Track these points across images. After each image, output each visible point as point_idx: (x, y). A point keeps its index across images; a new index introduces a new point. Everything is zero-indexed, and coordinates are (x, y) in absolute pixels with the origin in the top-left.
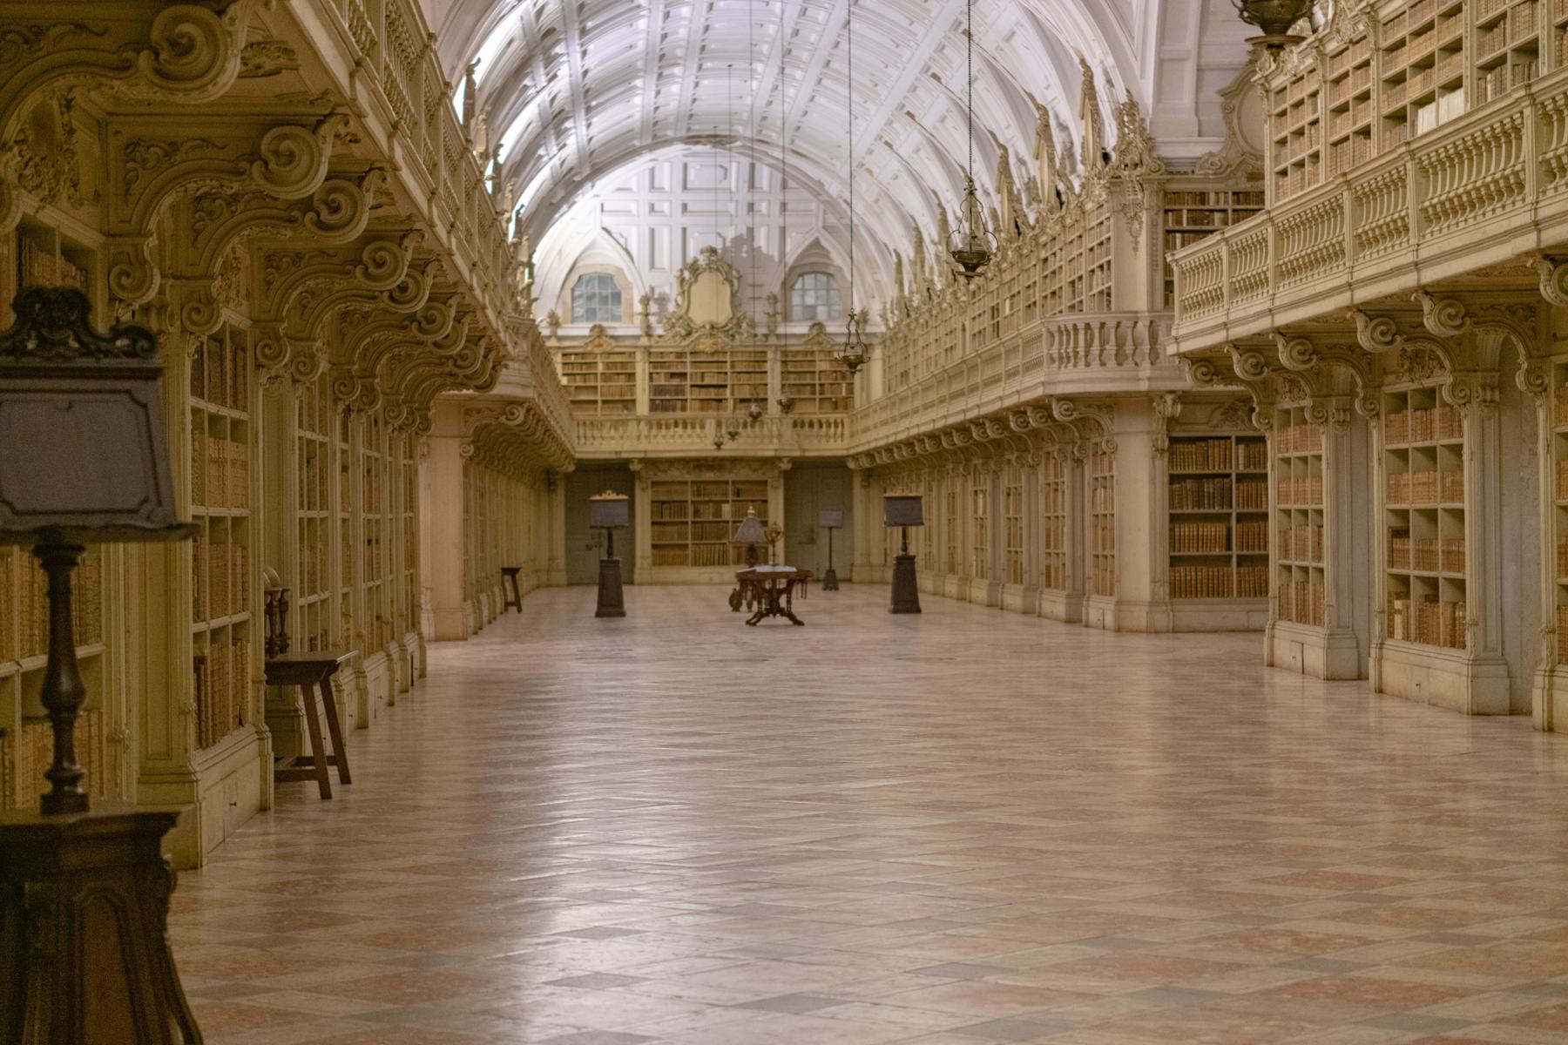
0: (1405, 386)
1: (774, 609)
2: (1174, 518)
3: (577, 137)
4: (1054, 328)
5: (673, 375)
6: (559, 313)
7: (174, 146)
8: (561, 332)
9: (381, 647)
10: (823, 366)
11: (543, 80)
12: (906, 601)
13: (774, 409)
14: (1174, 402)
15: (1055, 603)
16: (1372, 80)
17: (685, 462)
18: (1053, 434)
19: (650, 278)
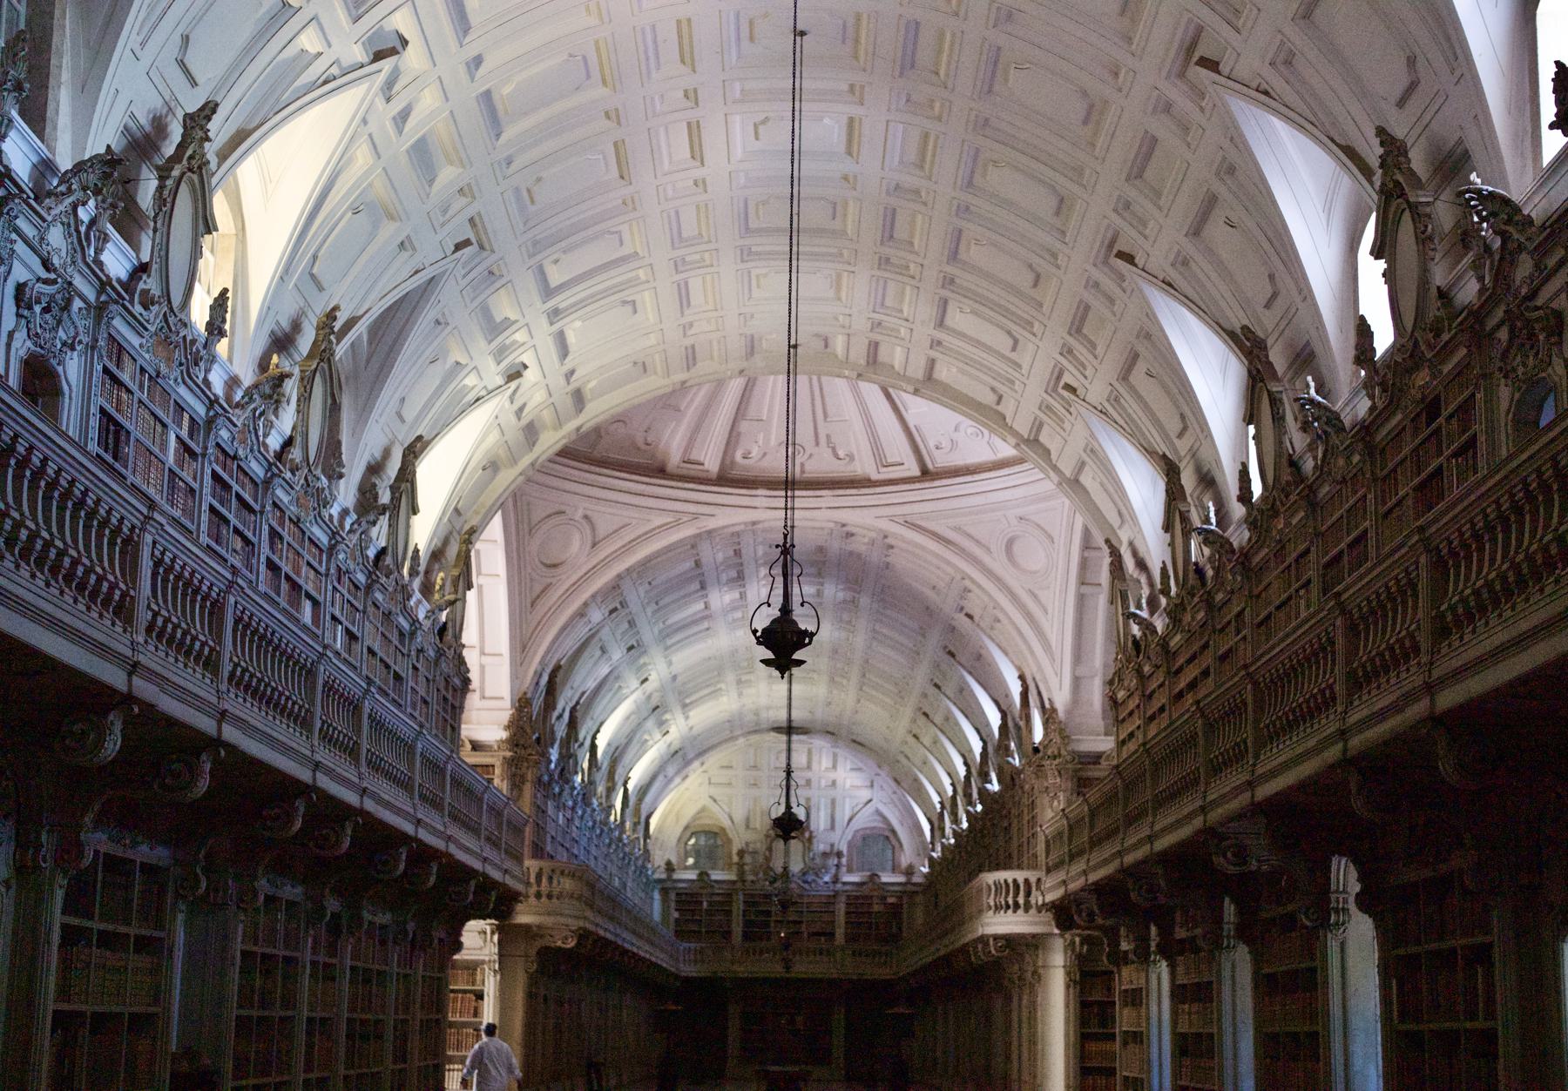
0: (1181, 933)
3: (679, 727)
4: (991, 882)
5: (763, 912)
6: (674, 860)
8: (676, 876)
10: (876, 908)
11: (635, 683)
14: (1082, 944)
19: (749, 836)
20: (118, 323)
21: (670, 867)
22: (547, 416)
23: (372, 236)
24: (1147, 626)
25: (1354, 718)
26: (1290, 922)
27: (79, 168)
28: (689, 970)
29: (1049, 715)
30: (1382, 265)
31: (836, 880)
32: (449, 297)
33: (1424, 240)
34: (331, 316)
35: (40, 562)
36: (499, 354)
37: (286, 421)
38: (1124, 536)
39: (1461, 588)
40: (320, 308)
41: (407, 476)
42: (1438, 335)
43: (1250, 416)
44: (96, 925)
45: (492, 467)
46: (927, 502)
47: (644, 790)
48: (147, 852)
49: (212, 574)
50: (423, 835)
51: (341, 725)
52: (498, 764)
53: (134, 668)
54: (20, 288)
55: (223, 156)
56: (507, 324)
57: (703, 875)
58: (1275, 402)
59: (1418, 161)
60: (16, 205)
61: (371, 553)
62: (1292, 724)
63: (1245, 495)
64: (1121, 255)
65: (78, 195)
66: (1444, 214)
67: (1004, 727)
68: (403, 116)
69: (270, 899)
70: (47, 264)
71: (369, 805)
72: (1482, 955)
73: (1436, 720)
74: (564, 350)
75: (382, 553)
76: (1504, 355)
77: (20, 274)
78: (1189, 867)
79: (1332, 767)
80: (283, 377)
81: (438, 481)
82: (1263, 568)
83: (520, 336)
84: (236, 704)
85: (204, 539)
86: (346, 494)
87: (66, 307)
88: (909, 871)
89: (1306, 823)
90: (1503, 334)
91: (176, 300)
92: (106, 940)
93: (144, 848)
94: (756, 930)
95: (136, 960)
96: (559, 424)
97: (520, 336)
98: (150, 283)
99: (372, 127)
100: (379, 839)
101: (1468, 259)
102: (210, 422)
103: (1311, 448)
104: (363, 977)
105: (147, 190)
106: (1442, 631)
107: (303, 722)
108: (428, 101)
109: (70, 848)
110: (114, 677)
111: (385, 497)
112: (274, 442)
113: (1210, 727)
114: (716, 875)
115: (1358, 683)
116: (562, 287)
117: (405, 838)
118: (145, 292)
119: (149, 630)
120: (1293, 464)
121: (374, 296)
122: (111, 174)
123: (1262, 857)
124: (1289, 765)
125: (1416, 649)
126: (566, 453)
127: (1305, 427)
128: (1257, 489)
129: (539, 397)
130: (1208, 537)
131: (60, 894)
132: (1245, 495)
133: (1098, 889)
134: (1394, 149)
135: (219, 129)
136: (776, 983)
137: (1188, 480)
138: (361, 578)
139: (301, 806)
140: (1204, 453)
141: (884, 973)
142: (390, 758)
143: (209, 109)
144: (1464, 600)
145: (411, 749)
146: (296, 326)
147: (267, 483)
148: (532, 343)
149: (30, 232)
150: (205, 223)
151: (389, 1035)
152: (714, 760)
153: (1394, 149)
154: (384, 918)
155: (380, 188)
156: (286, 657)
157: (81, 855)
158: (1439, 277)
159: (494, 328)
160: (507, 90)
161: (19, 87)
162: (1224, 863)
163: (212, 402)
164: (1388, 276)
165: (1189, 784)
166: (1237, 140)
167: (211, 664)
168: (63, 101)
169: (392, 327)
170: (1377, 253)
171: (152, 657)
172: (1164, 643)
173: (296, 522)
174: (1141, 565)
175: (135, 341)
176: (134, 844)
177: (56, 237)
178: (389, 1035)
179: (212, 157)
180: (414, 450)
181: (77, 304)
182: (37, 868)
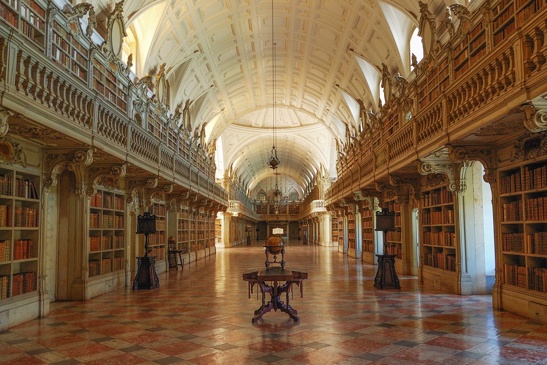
0: (349, 211)
2: (333, 230)
7: (136, 182)
13: (288, 213)
24: (343, 155)
26: (368, 209)
27: (142, 79)
28: (259, 220)
30: (383, 89)
31: (287, 202)
32: (209, 96)
33: (390, 85)
35: (142, 153)
37: (181, 121)
38: (339, 137)
39: (394, 151)
40: (186, 99)
41: (203, 130)
43: (361, 116)
46: (302, 131)
49: (171, 153)
50: (210, 197)
51: (194, 179)
52: (222, 182)
54: (134, 102)
57: (261, 201)
58: (365, 114)
59: (389, 70)
61: (197, 145)
62: (366, 175)
63: (360, 131)
66: (394, 80)
67: (317, 173)
70: (138, 97)
71: (200, 192)
73: (389, 174)
77: (133, 99)
78: (349, 199)
81: (208, 130)
84: (177, 176)
85: (168, 145)
86: (192, 134)
88: (300, 200)
89: (368, 192)
90: (403, 103)
91: (161, 101)
98: (156, 98)
100: (202, 199)
102: (168, 123)
103: (371, 122)
105: (154, 81)
109: (148, 202)
110: (156, 173)
111: (199, 135)
112: (179, 126)
113: (352, 174)
116: (231, 93)
117: (206, 198)
123: (362, 198)
124: (366, 182)
128: (362, 130)
130: (353, 138)
132: (360, 131)
133: (334, 203)
134: (385, 67)
136: (277, 222)
138: (196, 150)
140: (353, 122)
141: (296, 219)
142: (203, 183)
143: (164, 65)
146: (182, 103)
147: (178, 133)
149: (135, 91)
157: (150, 203)
158: (393, 92)
162: (356, 199)
164: (384, 91)
166: (357, 64)
167: (172, 169)
169: (199, 103)
173: (184, 140)
174: (342, 142)
175: (154, 109)
177: (139, 92)
179: (165, 73)
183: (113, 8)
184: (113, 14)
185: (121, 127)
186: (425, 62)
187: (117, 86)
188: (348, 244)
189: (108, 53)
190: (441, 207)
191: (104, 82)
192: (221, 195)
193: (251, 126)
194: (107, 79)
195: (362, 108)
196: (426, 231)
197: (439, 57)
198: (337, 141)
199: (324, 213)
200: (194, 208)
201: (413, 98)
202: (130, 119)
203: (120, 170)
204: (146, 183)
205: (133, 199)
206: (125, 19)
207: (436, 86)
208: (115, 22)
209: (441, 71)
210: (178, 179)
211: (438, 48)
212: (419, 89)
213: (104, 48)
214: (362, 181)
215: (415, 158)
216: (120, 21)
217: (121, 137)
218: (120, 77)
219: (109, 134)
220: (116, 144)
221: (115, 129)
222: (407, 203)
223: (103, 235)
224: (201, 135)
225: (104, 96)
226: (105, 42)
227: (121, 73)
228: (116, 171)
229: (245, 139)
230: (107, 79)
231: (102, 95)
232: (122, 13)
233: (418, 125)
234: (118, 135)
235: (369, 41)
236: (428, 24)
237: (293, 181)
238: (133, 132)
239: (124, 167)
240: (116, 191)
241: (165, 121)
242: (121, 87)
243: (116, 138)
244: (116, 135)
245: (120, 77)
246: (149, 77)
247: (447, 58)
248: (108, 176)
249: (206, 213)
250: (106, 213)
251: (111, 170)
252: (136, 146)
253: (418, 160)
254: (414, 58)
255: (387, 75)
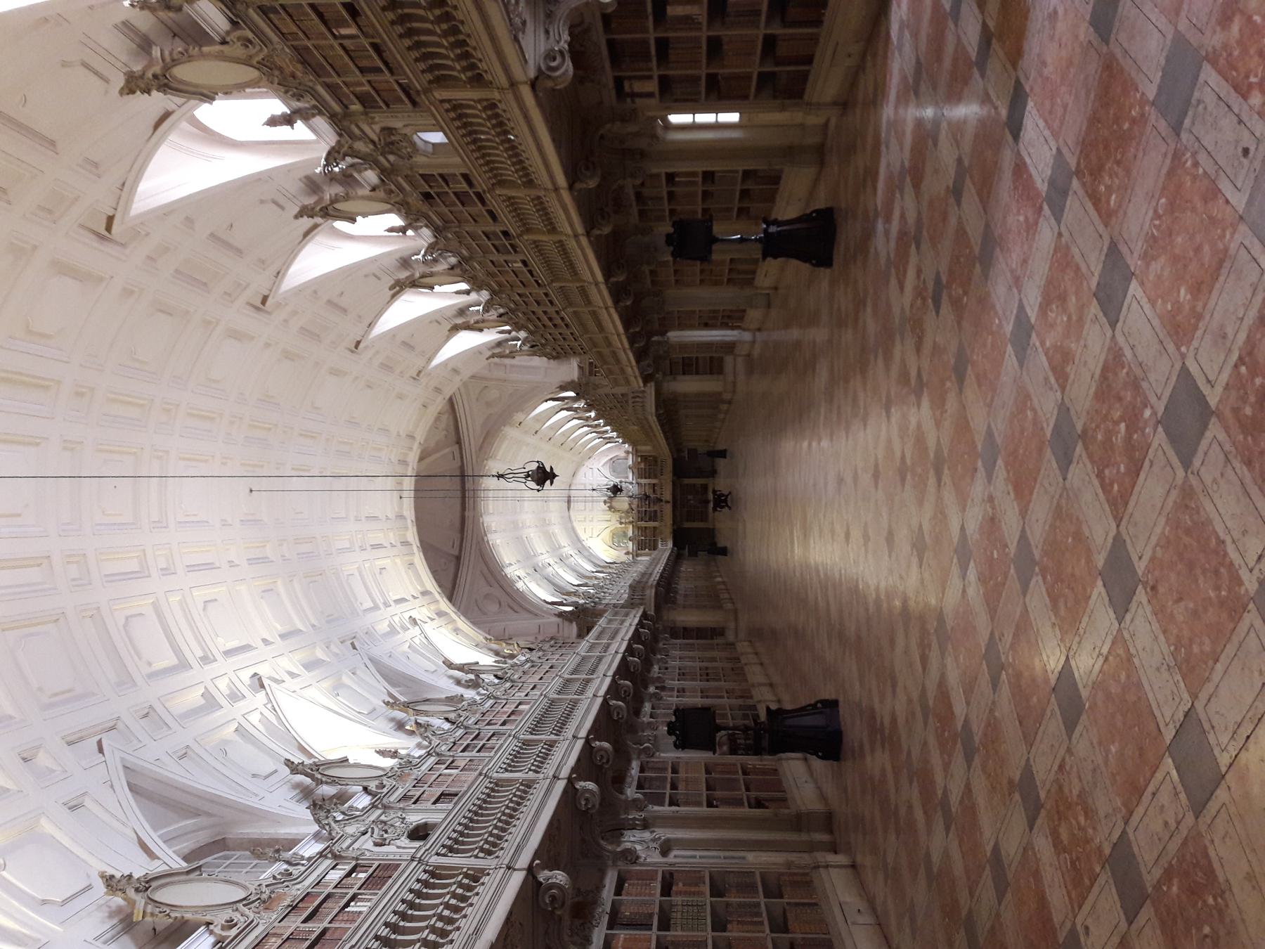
1: (725, 501)
2: (697, 373)
3: (568, 550)
9: (742, 668)
10: (642, 466)
12: (722, 454)
15: (724, 407)
16: (553, 331)
17: (674, 511)
18: (669, 412)
20: (392, 799)
21: (627, 553)
22: (433, 607)
23: (349, 687)
25: (569, 231)
27: (318, 821)
28: (670, 544)
29: (563, 388)
30: (359, 218)
32: (379, 651)
33: (347, 198)
34: (387, 703)
36: (405, 629)
37: (437, 722)
39: (510, 173)
41: (461, 668)
42: (391, 191)
44: (668, 791)
45: (457, 630)
47: (596, 565)
48: (634, 770)
49: (509, 745)
51: (576, 686)
53: (555, 777)
54: (376, 844)
55: (311, 756)
56: (390, 625)
58: (422, 277)
59: (310, 201)
60: (336, 848)
61: (496, 681)
62: (571, 266)
63: (467, 292)
64: (356, 347)
65: (330, 820)
67: (568, 409)
68: (293, 675)
69: (651, 717)
70: (364, 833)
71: (611, 673)
72: (671, 177)
73: (571, 187)
74: (403, 600)
75: (496, 676)
76: (400, 157)
79: (590, 242)
80: (417, 723)
82: (500, 285)
83: (396, 619)
86: (469, 694)
87: (385, 823)
88: (627, 452)
90: (392, 158)
92: (674, 786)
93: (633, 772)
94: (653, 517)
95: (682, 775)
96: (437, 601)
97: (396, 619)
98: (372, 786)
99: (297, 688)
100: (624, 669)
101: (356, 175)
102: (438, 754)
103: (445, 258)
104: (682, 675)
105: (328, 790)
106: (530, 183)
107: (575, 703)
108: (286, 663)
109: (636, 805)
110: (560, 786)
111: (472, 677)
112: (447, 726)
114: (630, 533)
115: (553, 229)
116: (373, 601)
117: (624, 659)
118: (377, 787)
119: (537, 772)
120: (452, 268)
121: (376, 684)
122: (318, 806)
125: (539, 198)
126: (450, 599)
127: (435, 261)
129: (424, 610)
131: (656, 808)
132: (467, 292)
135: (297, 758)
137: (459, 321)
139: (613, 702)
141: (670, 462)
142: (589, 666)
144: (517, 171)
145: (584, 658)
146: (392, 720)
147: (466, 728)
148: (400, 614)
149: (349, 841)
150: (344, 761)
151: (705, 664)
152: (583, 536)
153: (304, 212)
154: (656, 668)
155: (326, 684)
156: (547, 712)
158: (366, 191)
159: (393, 631)
160: (278, 627)
161: (278, 851)
163: (429, 754)
164: (365, 215)
165: (594, 314)
166: (300, 290)
167: (551, 744)
168: (285, 831)
169: (391, 676)
170: (353, 220)
171: (549, 770)
172: (531, 332)
173: (484, 714)
176: (631, 776)
177: (351, 829)
178: (705, 664)
180: (450, 665)
181: (383, 818)
182: (644, 819)
183: (118, 901)
184: (132, 903)
185: (434, 886)
186: (286, 85)
187: (329, 890)
188: (733, 328)
189: (237, 917)
190: (658, 40)
191: (316, 927)
192: (614, 626)
193: (458, 558)
194: (305, 921)
195: (414, 284)
196: (717, 97)
197: (265, 41)
198: (493, 356)
199: (658, 393)
200: (646, 688)
201: (377, 128)
202: (413, 859)
203: (553, 886)
204: (586, 812)
205: (628, 845)
206: (155, 868)
207: (342, 52)
208: (160, 896)
209: (301, 34)
210: (578, 728)
211: (239, 39)
212: (353, 107)
213: (223, 928)
214: (587, 276)
215: (526, 92)
216: (154, 884)
217: (461, 885)
218: (307, 883)
219: (450, 921)
220: (480, 901)
221: (437, 905)
222: (643, 154)
223: (724, 930)
224: (472, 671)
225: (353, 926)
226: (208, 924)
227: (297, 880)
228: (553, 897)
229: (486, 571)
230: (305, 921)
231: (350, 932)
232: (136, 876)
233: (441, 81)
234: (454, 895)
235: (239, 252)
236: (183, 72)
237: (583, 470)
238: (451, 849)
239: (543, 875)
240: (607, 894)
241: (432, 760)
242: (335, 876)
243: (463, 899)
244: (453, 902)
245: (307, 883)
246: (315, 805)
247: (264, 11)
248: (567, 921)
249: (659, 661)
250: (665, 925)
251: (552, 912)
252: (487, 842)
253: (533, 85)
254: (273, 122)
255: (323, 204)
